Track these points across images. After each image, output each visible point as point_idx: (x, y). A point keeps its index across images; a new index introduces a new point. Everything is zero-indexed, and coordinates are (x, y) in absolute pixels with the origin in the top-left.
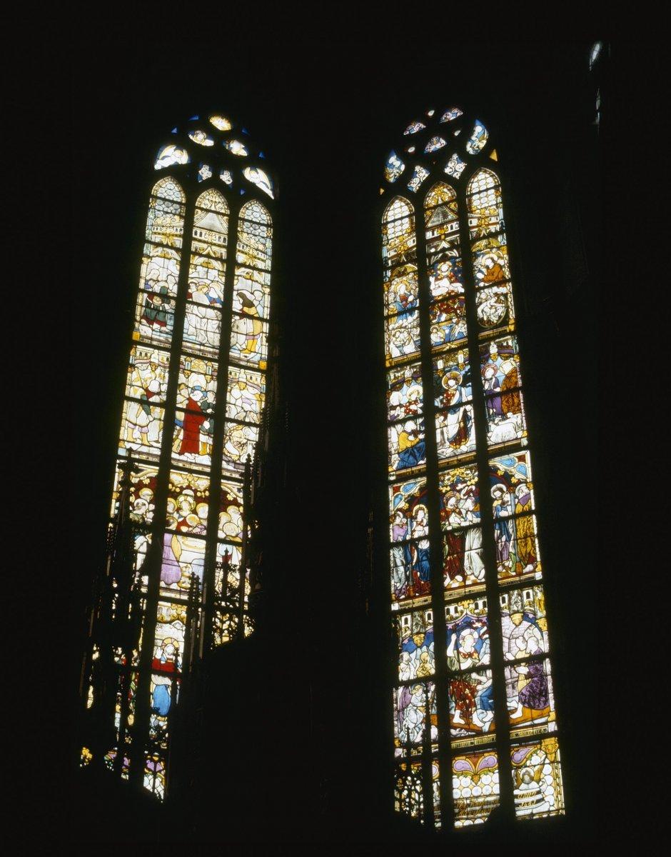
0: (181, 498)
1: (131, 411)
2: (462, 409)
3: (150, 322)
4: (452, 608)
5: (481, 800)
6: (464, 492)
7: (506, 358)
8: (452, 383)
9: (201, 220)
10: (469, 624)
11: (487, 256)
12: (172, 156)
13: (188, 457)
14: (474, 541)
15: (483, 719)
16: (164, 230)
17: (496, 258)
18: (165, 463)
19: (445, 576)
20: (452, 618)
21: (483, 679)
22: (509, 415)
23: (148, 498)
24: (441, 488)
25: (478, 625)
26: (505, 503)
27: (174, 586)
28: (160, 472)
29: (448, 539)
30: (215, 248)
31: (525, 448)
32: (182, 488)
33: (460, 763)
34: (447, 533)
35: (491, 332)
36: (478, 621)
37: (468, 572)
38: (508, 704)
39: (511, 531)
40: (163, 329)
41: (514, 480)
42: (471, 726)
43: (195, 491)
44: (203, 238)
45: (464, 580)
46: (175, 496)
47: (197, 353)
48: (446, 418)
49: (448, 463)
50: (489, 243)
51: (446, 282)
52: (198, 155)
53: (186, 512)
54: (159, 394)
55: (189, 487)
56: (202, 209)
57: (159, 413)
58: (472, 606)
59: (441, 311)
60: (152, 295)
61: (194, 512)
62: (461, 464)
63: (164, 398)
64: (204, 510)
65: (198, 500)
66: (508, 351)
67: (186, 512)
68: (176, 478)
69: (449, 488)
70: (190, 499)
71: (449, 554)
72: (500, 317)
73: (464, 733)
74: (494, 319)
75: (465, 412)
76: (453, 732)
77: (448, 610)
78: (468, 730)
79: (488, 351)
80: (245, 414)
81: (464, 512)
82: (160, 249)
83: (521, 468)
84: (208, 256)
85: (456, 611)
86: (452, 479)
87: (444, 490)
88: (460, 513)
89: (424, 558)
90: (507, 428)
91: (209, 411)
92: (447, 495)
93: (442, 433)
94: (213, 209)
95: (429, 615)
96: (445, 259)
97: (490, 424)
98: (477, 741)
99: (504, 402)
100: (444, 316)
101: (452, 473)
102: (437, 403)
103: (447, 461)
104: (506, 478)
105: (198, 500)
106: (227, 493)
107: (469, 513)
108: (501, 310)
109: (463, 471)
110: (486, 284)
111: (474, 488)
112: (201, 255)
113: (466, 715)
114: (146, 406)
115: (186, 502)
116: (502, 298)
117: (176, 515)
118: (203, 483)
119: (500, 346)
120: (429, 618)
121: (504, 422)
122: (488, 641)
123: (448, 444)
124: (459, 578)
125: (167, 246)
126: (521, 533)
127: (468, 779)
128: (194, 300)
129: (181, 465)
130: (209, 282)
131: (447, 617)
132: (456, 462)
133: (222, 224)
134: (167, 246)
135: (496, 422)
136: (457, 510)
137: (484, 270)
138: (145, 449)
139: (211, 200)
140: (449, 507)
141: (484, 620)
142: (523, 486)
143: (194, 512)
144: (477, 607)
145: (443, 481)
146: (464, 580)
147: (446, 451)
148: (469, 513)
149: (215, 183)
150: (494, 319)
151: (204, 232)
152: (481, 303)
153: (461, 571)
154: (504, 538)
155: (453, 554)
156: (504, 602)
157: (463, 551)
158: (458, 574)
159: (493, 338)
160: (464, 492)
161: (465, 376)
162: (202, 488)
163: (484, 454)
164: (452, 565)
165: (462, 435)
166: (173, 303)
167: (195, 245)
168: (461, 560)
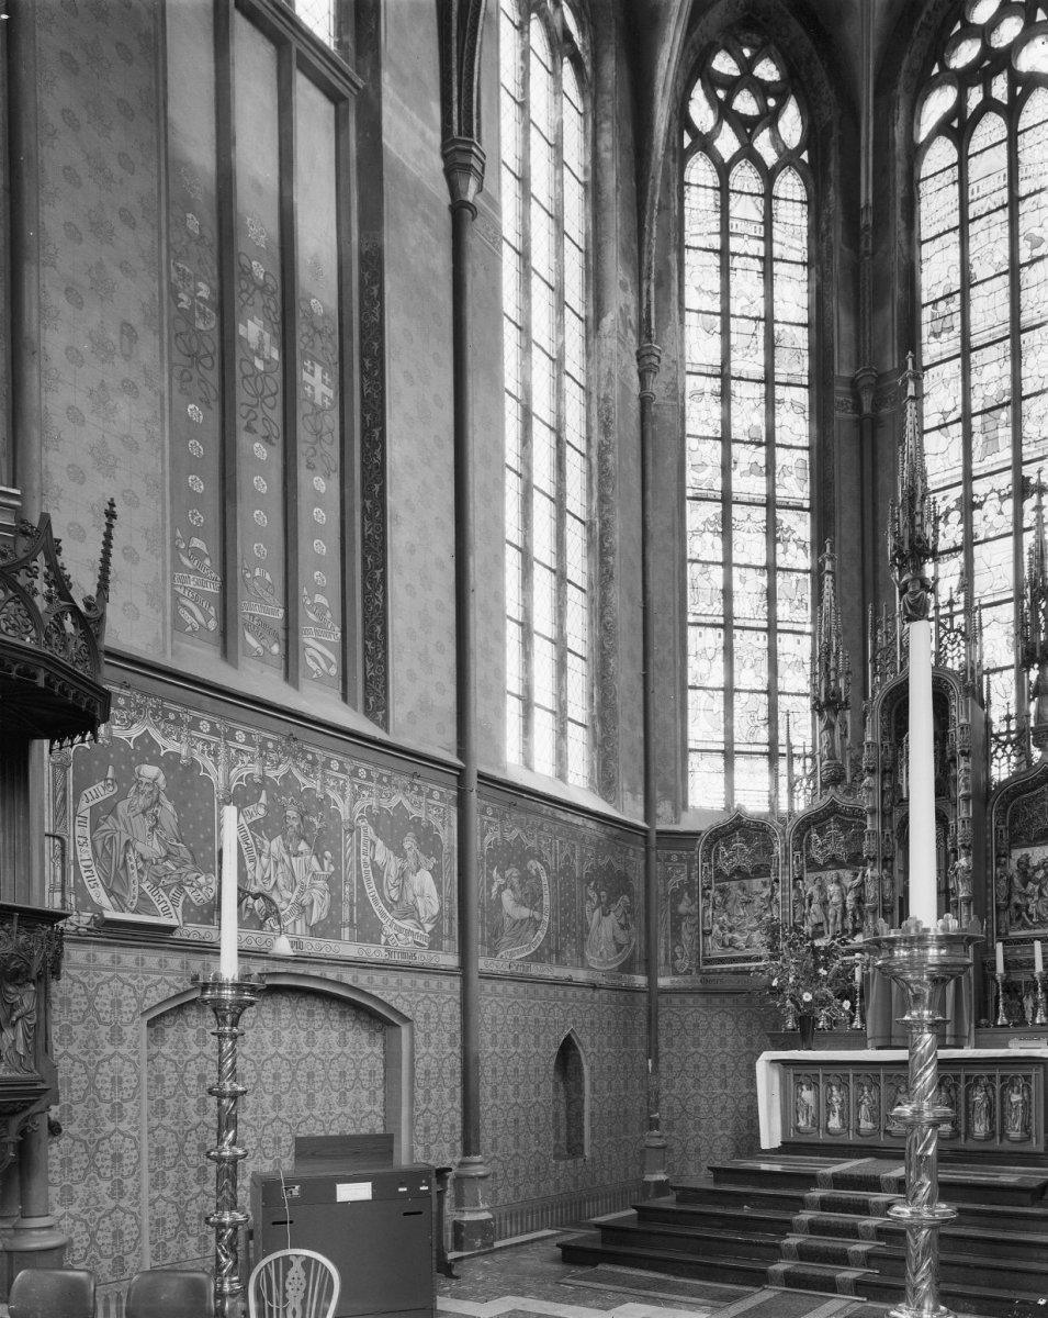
0: (985, 506)
1: (932, 442)
3: (936, 335)
9: (976, 168)
12: (940, 103)
13: (990, 460)
16: (938, 215)
18: (969, 478)
23: (957, 520)
27: (989, 592)
28: (965, 488)
30: (994, 196)
32: (986, 495)
40: (953, 334)
43: (999, 492)
44: (980, 195)
46: (979, 506)
47: (987, 341)
52: (964, 79)
53: (992, 517)
54: (955, 409)
55: (993, 490)
56: (975, 155)
57: (958, 429)
60: (935, 302)
61: (1001, 513)
63: (960, 410)
64: (1009, 505)
65: (1002, 498)
67: (992, 517)
68: (979, 488)
70: (996, 502)
80: (1041, 381)
82: (937, 241)
84: (989, 213)
91: (1006, 399)
94: (989, 143)
105: (1002, 498)
106: (1029, 478)
112: (980, 217)
114: (944, 430)
115: (990, 507)
117: (983, 524)
118: (1005, 481)
125: (945, 232)
128: (979, 279)
129: (982, 472)
130: (991, 246)
133: (1000, 157)
134: (945, 232)
138: (948, 474)
139: (992, 128)
143: (1001, 513)
149: (989, 105)
151: (980, 183)
162: (1005, 486)
166: (958, 296)
167: (973, 210)
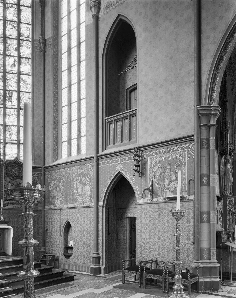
2: (14, 58)
4: (8, 109)
5: (12, 154)
6: (13, 81)
7: (28, 48)
8: (12, 49)
10: (12, 115)
11: (25, 13)
14: (15, 94)
15: (14, 137)
17: (28, 15)
19: (7, 101)
20: (8, 112)
21: (15, 128)
22: (27, 65)
24: (7, 78)
25: (14, 115)
26: (23, 88)
29: (8, 92)
31: (30, 75)
33: (7, 145)
34: (8, 90)
35: (24, 38)
36: (15, 114)
37: (13, 102)
38: (20, 135)
39: (25, 95)
41: (27, 83)
42: (11, 138)
45: (12, 104)
48: (9, 58)
49: (9, 72)
50: (26, 9)
51: (12, 15)
58: (13, 111)
59: (10, 24)
62: (13, 73)
66: (28, 46)
69: (9, 79)
71: (8, 96)
72: (27, 35)
73: (9, 139)
74: (26, 35)
75: (15, 59)
76: (6, 138)
77: (7, 110)
78: (10, 139)
79: (23, 44)
81: (13, 86)
83: (28, 80)
85: (9, 111)
86: (10, 76)
87: (8, 79)
88: (12, 86)
89: (1, 95)
90: (26, 68)
92: (9, 80)
93: (8, 62)
95: (2, 110)
96: (12, 7)
97: (22, 65)
98: (12, 142)
99: (26, 61)
100: (11, 27)
101: (10, 75)
102: (7, 53)
103: (9, 71)
104: (25, 82)
107: (14, 87)
108: (28, 33)
109: (13, 75)
110: (24, 23)
111: (16, 81)
113: (10, 135)
116: (28, 29)
119: (26, 44)
120: (2, 111)
121: (25, 66)
122: (17, 120)
123: (9, 66)
124: (10, 103)
126: (27, 97)
127: (10, 149)
131: (7, 111)
132: (12, 72)
135: (23, 65)
136: (11, 85)
137: (24, 17)
140: (9, 84)
141: (16, 115)
142: (29, 85)
144: (14, 111)
145: (8, 76)
146: (12, 104)
147: (9, 68)
148: (14, 87)
150: (26, 35)
152: (22, 28)
153: (11, 101)
154: (23, 97)
155: (9, 96)
156: (21, 112)
157: (12, 96)
158: (10, 101)
159: (25, 41)
160: (13, 81)
161: (16, 48)
163: (19, 73)
164: (9, 99)
165: (13, 65)
168: (11, 99)
